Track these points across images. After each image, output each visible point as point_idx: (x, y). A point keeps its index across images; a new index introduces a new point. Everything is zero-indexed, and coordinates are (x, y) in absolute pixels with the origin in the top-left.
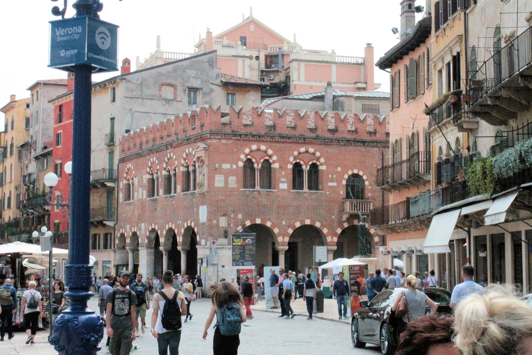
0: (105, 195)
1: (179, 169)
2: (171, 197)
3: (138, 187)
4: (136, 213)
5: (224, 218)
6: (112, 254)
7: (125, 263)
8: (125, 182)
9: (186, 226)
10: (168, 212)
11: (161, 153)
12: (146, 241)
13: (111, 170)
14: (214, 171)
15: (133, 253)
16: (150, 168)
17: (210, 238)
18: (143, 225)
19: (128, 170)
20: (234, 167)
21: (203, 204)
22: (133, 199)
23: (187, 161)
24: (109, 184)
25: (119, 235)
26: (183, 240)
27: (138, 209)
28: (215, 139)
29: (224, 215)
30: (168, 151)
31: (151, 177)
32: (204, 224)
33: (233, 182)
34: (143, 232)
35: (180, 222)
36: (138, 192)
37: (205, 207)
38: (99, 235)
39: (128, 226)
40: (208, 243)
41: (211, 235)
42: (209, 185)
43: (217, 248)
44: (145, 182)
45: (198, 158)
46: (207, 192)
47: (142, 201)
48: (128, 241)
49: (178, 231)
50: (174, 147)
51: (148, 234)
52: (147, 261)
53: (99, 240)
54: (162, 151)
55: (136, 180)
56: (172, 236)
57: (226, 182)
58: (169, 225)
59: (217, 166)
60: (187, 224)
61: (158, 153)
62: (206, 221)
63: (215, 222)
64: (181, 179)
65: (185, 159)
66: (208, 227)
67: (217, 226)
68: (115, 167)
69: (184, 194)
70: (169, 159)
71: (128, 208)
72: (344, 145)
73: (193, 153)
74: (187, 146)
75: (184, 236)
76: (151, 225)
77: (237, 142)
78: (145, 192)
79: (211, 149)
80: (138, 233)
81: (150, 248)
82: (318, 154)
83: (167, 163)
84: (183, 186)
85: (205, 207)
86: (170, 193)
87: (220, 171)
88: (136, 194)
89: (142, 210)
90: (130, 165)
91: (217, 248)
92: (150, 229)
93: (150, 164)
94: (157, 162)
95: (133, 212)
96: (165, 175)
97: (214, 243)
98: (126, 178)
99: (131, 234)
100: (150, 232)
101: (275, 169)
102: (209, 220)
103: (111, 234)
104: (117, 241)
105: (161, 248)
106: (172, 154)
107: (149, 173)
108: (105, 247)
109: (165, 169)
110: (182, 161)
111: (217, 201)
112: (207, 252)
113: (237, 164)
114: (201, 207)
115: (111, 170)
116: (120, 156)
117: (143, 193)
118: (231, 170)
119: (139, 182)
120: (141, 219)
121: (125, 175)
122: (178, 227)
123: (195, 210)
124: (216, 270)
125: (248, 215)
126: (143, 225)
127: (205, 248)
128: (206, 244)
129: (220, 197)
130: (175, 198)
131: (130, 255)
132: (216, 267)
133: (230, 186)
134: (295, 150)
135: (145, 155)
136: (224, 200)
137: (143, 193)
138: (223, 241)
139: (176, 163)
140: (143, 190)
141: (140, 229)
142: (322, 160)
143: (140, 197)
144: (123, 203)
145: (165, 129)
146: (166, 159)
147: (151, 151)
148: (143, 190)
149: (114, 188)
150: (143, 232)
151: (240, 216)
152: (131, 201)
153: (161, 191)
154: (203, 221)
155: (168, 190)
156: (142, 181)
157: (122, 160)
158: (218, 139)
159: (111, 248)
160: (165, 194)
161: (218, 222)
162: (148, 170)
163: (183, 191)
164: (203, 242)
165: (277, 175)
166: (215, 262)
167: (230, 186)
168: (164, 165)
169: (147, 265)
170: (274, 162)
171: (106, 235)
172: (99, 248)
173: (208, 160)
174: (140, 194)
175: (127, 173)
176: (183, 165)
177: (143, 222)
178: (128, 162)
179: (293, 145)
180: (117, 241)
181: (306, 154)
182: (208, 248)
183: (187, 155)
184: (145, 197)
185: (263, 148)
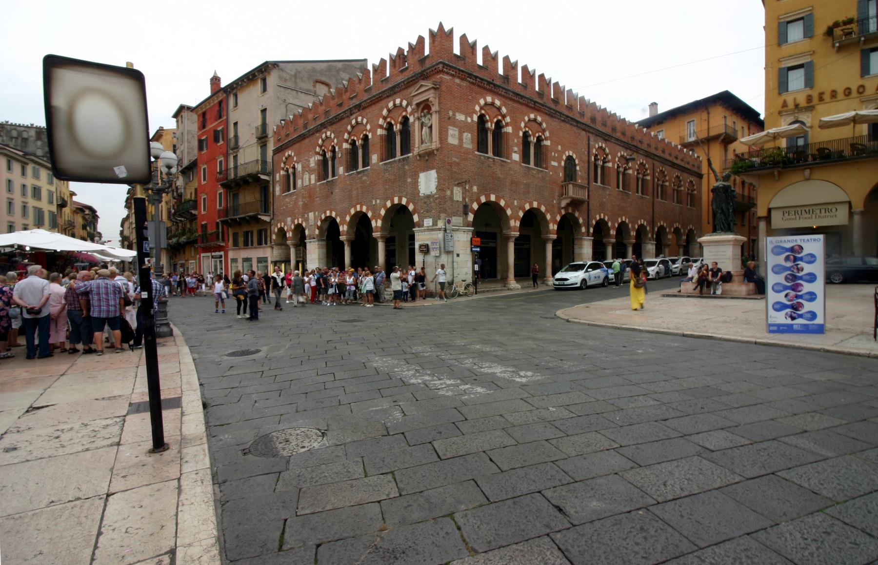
0: (258, 189)
1: (374, 133)
2: (359, 173)
3: (303, 174)
4: (301, 203)
5: (459, 189)
6: (269, 250)
7: (284, 259)
8: (282, 173)
9: (389, 204)
10: (354, 192)
11: (339, 124)
12: (317, 232)
13: (264, 162)
14: (446, 121)
16: (321, 147)
17: (443, 215)
18: (311, 215)
20: (469, 120)
21: (426, 169)
22: (295, 188)
23: (389, 120)
24: (263, 177)
25: (276, 230)
26: (383, 224)
27: (303, 197)
28: (448, 73)
29: (458, 185)
30: (354, 116)
31: (320, 158)
32: (428, 197)
33: (469, 140)
34: (311, 222)
35: (378, 201)
36: (302, 179)
37: (433, 173)
38: (252, 233)
39: (289, 219)
40: (441, 224)
41: (445, 211)
42: (441, 139)
43: (453, 230)
44: (312, 164)
45: (418, 105)
46: (437, 150)
47: (309, 189)
48: (289, 235)
49: (373, 213)
50: (364, 108)
51: (319, 223)
53: (252, 237)
54: (342, 119)
55: (299, 167)
56: (362, 222)
57: (461, 139)
58: (356, 209)
59: (451, 113)
60: (392, 201)
61: (334, 126)
62: (434, 191)
63: (448, 193)
64: (379, 146)
65: (385, 118)
66: (437, 201)
67: (451, 198)
68: (269, 159)
70: (353, 127)
71: (287, 200)
72: (564, 121)
73: (405, 103)
74: (390, 98)
75: (384, 219)
76: (325, 213)
77: (472, 86)
78: (313, 177)
79: (443, 88)
80: (304, 225)
81: (322, 240)
82: (544, 125)
83: (349, 133)
84: (382, 154)
85: (433, 173)
86: (356, 167)
87: (452, 121)
88: (299, 182)
89: (310, 197)
91: (453, 230)
92: (323, 217)
93: (320, 142)
94: (333, 136)
95: (296, 203)
96: (346, 149)
97: (449, 222)
98: (283, 169)
99: (293, 227)
100: (322, 221)
101: (508, 134)
102: (440, 188)
103: (266, 230)
104: (274, 237)
106: (360, 119)
107: (318, 153)
108: (260, 243)
109: (347, 141)
110: (381, 121)
111: (451, 164)
112: (440, 235)
113: (472, 118)
114: (422, 176)
115: (264, 162)
117: (310, 179)
118: (466, 122)
119: (303, 167)
120: (307, 208)
121: (282, 165)
122: (375, 209)
123: (409, 180)
124: (450, 260)
125: (484, 190)
127: (433, 230)
128: (435, 223)
129: (454, 159)
131: (292, 251)
132: (450, 256)
133: (465, 146)
134: (525, 115)
135: (313, 134)
136: (458, 164)
137: (310, 179)
138: (457, 220)
139: (368, 127)
140: (310, 174)
141: (307, 220)
142: (547, 134)
143: (307, 183)
144: (280, 195)
145: (346, 91)
146: (349, 128)
147: (323, 126)
148: (310, 174)
149: (268, 182)
150: (311, 222)
151: (475, 189)
152: (292, 191)
153: (341, 170)
154: (428, 193)
155: (352, 164)
156: (308, 165)
157: (278, 151)
158: (452, 75)
159: (266, 243)
160: (348, 170)
161: (452, 193)
162: (318, 149)
163: (382, 160)
164: (428, 222)
165: (511, 143)
166: (451, 249)
167: (465, 146)
168: (346, 136)
169: (319, 259)
170: (507, 124)
171: (260, 232)
172: (252, 244)
173: (440, 103)
174: (307, 179)
175: (285, 163)
176: (381, 127)
179: (524, 108)
180: (274, 237)
181: (533, 124)
182: (440, 229)
183: (389, 111)
184: (313, 182)
185: (498, 103)
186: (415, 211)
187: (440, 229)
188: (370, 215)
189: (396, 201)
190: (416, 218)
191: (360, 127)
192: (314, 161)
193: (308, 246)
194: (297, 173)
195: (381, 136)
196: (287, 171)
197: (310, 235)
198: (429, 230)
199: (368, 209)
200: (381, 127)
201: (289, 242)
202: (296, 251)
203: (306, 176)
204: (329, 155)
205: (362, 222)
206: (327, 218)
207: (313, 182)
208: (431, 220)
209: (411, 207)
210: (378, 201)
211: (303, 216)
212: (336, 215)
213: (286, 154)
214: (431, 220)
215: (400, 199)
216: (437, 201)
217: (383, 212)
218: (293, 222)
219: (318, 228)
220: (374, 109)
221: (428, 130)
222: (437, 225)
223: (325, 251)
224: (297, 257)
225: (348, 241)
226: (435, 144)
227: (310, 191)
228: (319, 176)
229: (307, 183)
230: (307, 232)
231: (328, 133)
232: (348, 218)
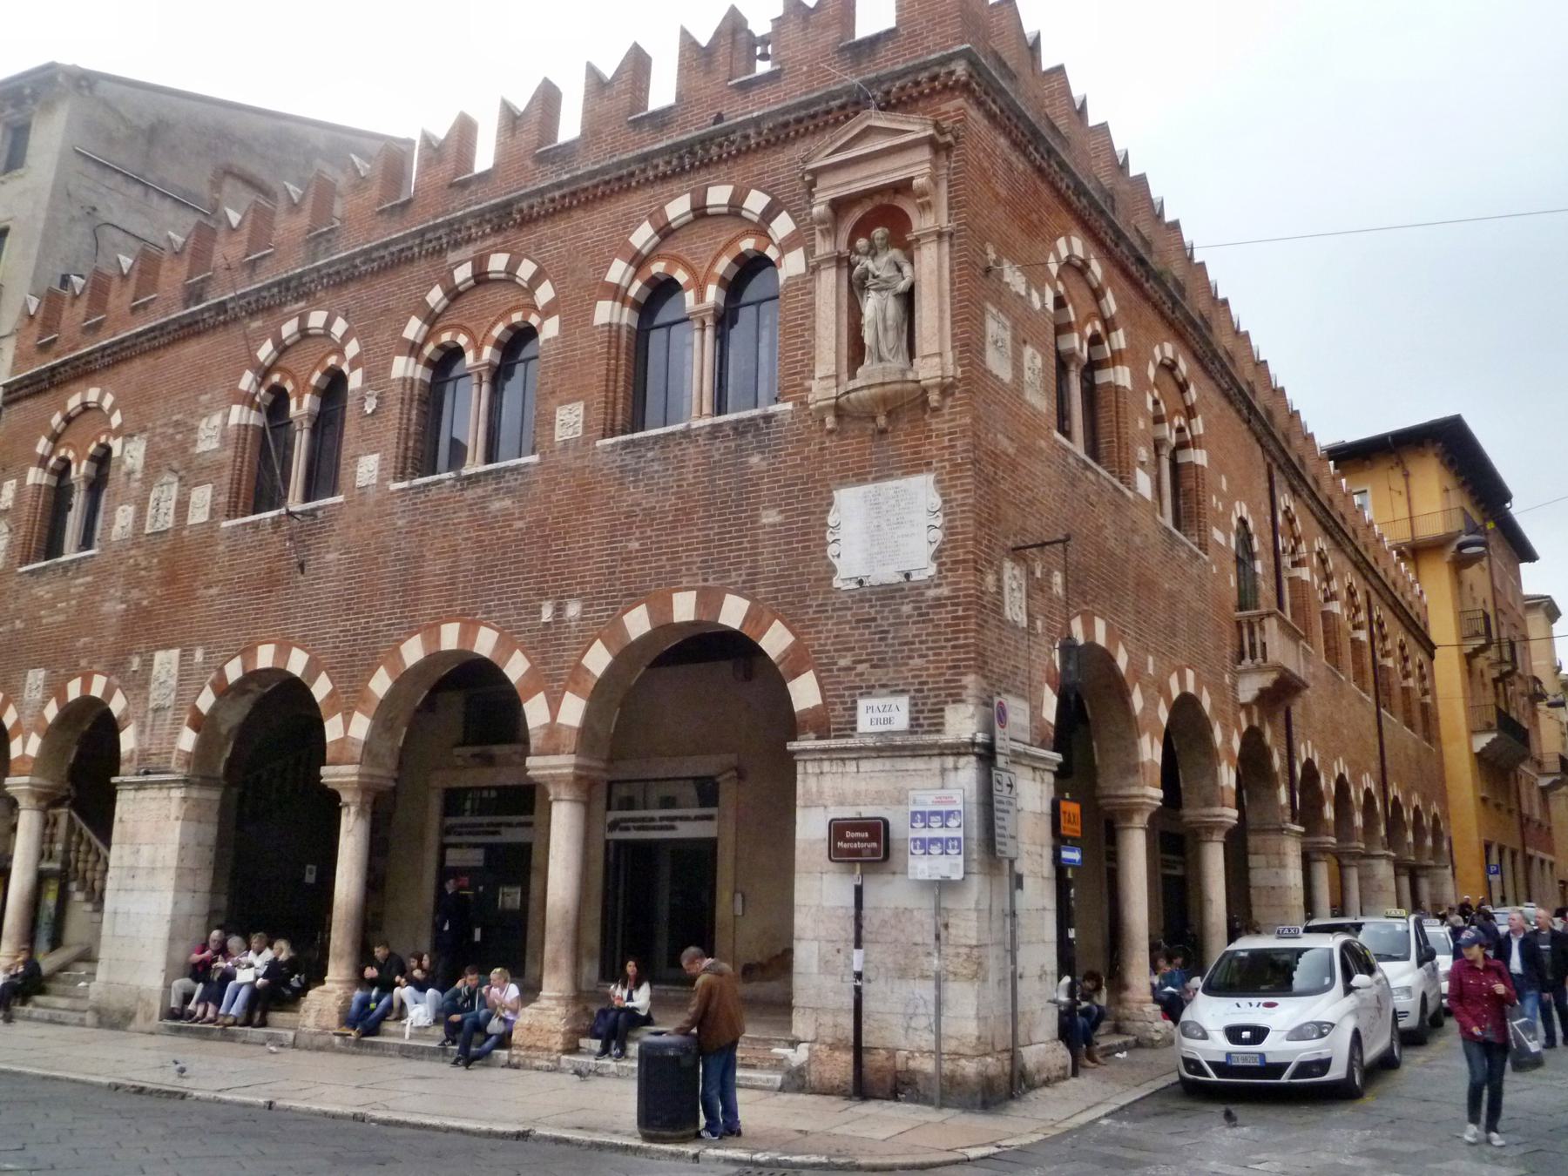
8: (35, 476)
12: (188, 740)
15: (44, 811)
19: (68, 420)
22: (86, 542)
32: (888, 593)
40: (962, 723)
51: (206, 701)
52: (182, 847)
55: (131, 454)
66: (943, 616)
69: (626, 445)
71: (43, 591)
76: (249, 652)
80: (117, 705)
84: (610, 404)
89: (170, 579)
90: (93, 395)
92: (234, 671)
99: (51, 712)
100: (224, 692)
105: (331, 775)
107: (248, 400)
116: (13, 373)
117: (182, 507)
120: (144, 629)
121: (42, 446)
126: (166, 662)
130: (511, 481)
137: (182, 507)
140: (186, 485)
141: (139, 684)
143: (169, 521)
154: (888, 574)
155: (425, 448)
162: (247, 381)
164: (880, 714)
169: (181, 873)
176: (616, 293)
177: (168, 647)
178: (82, 384)
186: (798, 660)
187: (958, 750)
188: (516, 668)
189: (684, 608)
190: (805, 693)
191: (496, 297)
192: (220, 427)
193: (127, 806)
194: (116, 476)
195: (612, 329)
196: (64, 467)
197: (144, 756)
198: (888, 749)
199: (507, 644)
200: (616, 293)
201: (17, 784)
202: (48, 824)
203: (166, 493)
204: (302, 407)
205: (471, 702)
206: (251, 677)
207: (198, 516)
208: (903, 702)
209: (775, 641)
210: (573, 609)
211: (116, 667)
212: (313, 668)
213: (74, 402)
214: (903, 702)
215: (710, 600)
216: (943, 616)
217: (598, 659)
218: (55, 689)
219: (199, 722)
220: (593, 223)
221: (893, 308)
222: (938, 727)
223: (211, 832)
224: (44, 854)
225: (364, 789)
226: (934, 362)
227: (177, 560)
228: (235, 494)
229: (169, 521)
230: (128, 741)
231: (317, 319)
232: (381, 684)
